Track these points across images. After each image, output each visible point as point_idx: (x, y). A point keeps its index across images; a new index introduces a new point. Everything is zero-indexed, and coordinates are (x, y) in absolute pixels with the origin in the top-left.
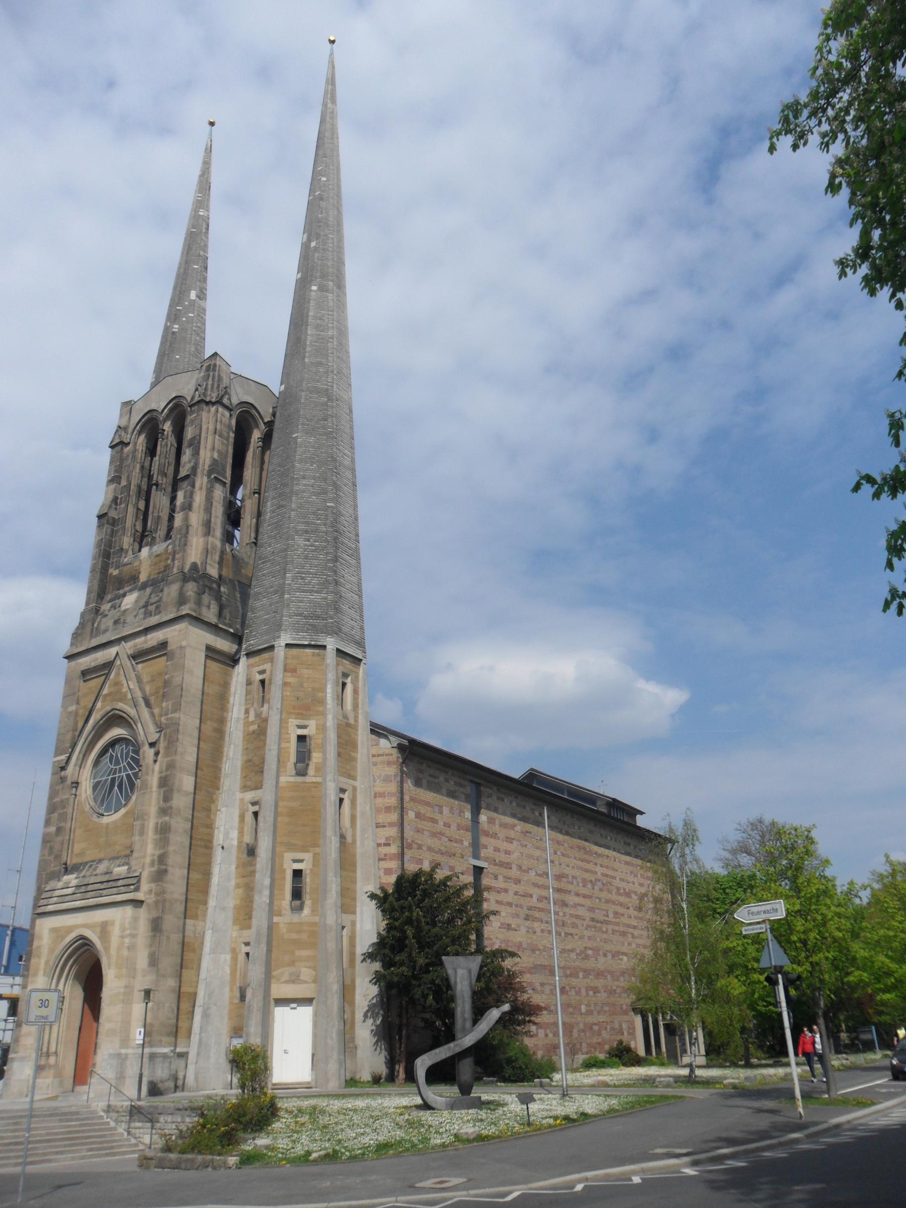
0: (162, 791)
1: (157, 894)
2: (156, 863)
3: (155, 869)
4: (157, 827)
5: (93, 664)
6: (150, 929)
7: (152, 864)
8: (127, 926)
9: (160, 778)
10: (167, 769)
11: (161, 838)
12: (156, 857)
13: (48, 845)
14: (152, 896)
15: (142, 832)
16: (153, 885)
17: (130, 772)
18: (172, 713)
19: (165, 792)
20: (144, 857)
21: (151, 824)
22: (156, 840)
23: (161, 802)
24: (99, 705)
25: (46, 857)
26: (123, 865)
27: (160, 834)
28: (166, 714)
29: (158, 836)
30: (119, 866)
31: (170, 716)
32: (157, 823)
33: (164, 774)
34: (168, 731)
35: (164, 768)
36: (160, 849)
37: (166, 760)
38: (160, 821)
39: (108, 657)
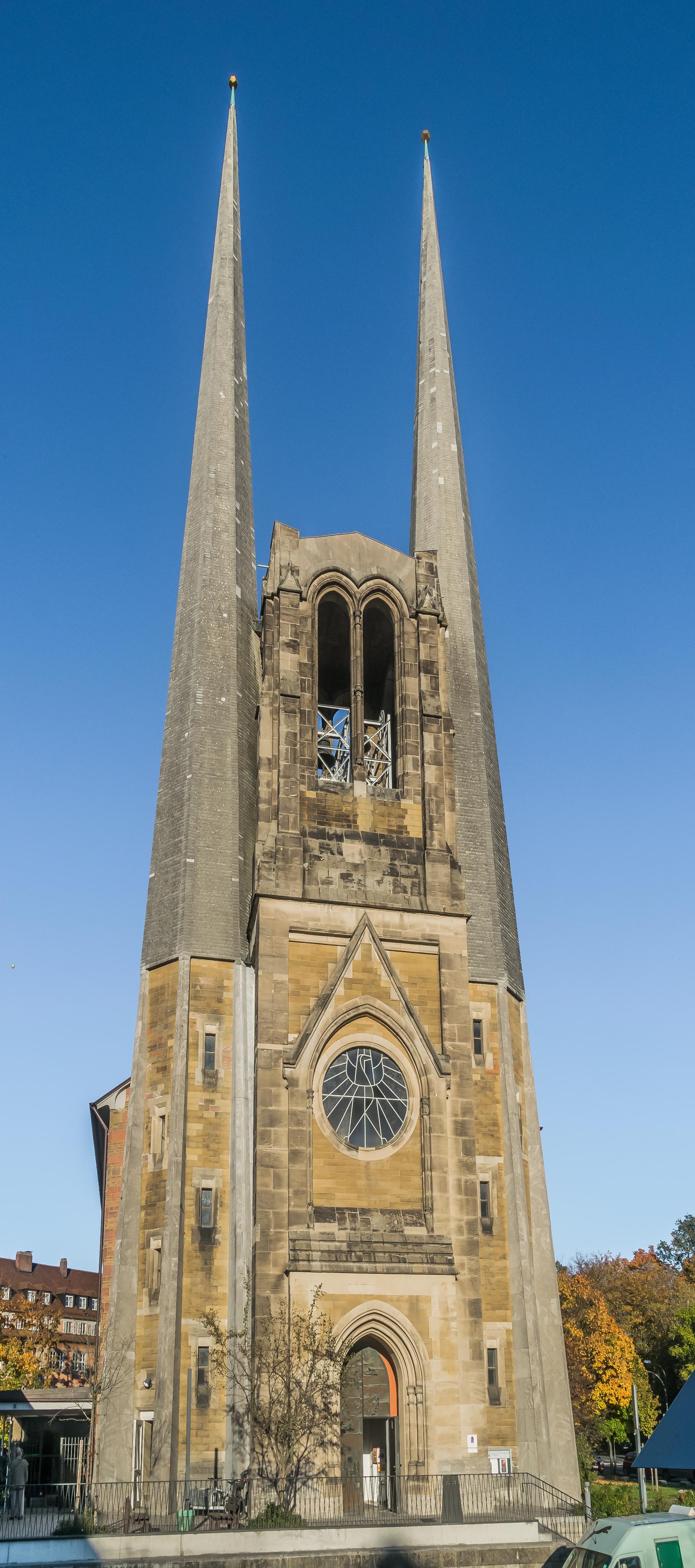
0: (461, 1138)
1: (470, 1270)
2: (465, 1231)
3: (465, 1237)
4: (459, 1185)
5: (311, 925)
6: (468, 1313)
7: (460, 1230)
8: (451, 1306)
9: (456, 1122)
10: (464, 1114)
11: (468, 1200)
12: (463, 1223)
13: (272, 1170)
14: (466, 1271)
15: (444, 1188)
16: (465, 1259)
17: (386, 1099)
18: (460, 1040)
19: (464, 1142)
20: (448, 1220)
21: (451, 1180)
22: (461, 1201)
23: (462, 1154)
24: (340, 990)
25: (271, 1188)
26: (415, 1224)
27: (466, 1195)
28: (454, 1040)
29: (463, 1197)
30: (407, 1224)
31: (457, 1043)
32: (459, 1180)
33: (460, 1118)
34: (459, 1062)
35: (459, 1112)
36: (468, 1214)
37: (460, 1100)
38: (463, 1178)
39: (339, 924)
